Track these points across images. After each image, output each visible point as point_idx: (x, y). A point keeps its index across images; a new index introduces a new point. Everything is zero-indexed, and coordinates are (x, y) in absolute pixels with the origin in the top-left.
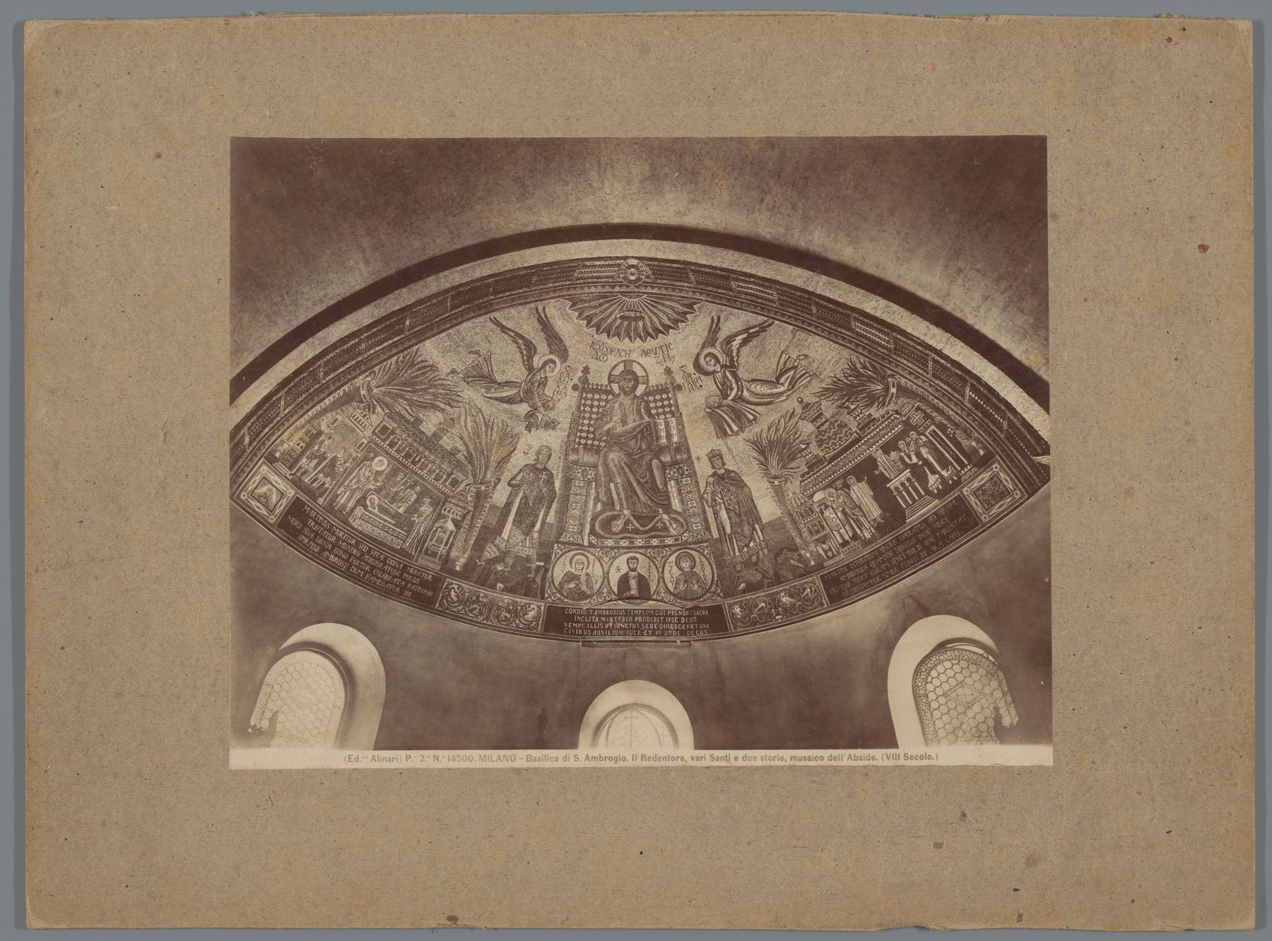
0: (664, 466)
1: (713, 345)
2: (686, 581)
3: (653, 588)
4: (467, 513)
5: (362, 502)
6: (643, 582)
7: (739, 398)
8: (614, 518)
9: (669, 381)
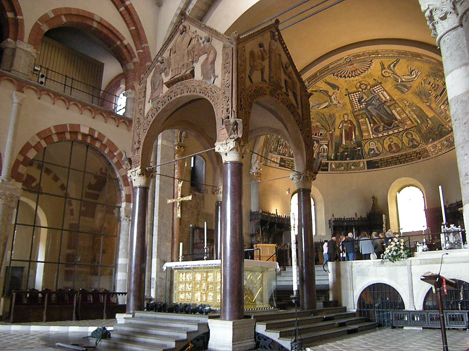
0: (389, 106)
2: (411, 142)
3: (400, 145)
4: (329, 142)
6: (397, 145)
7: (402, 81)
8: (379, 127)
9: (376, 82)
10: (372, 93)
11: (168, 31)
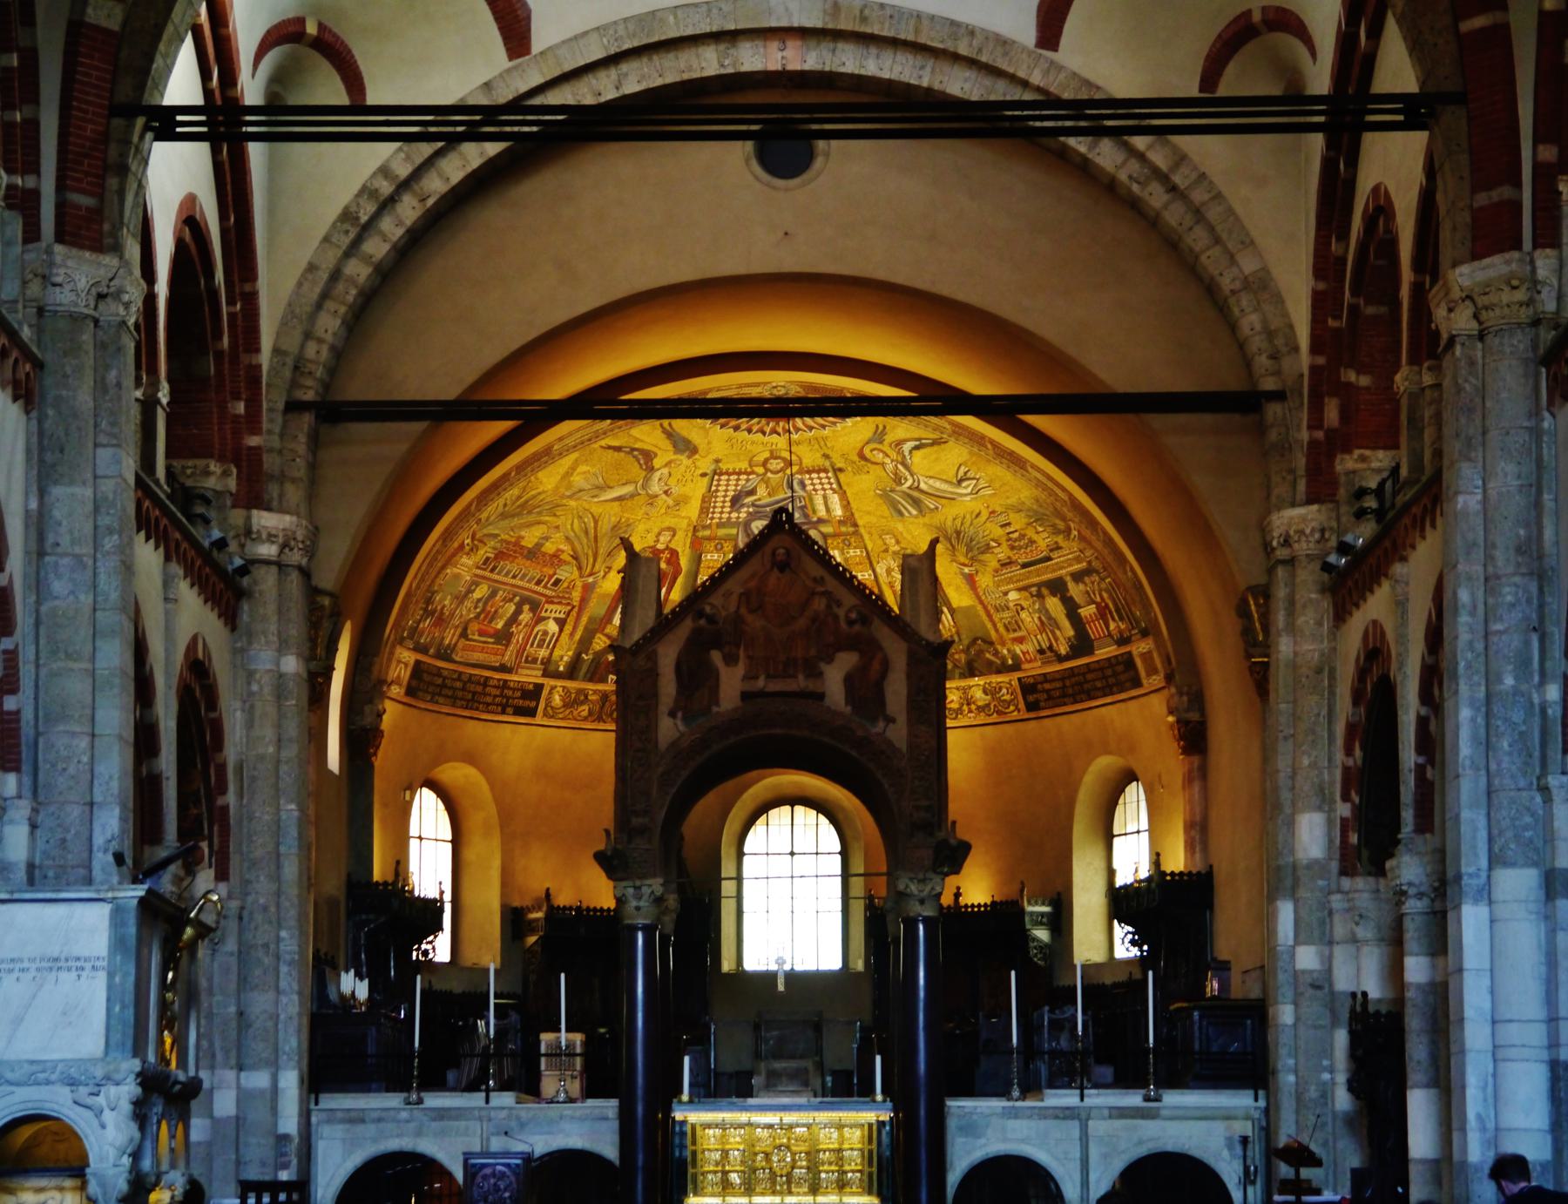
1: (881, 442)
5: (464, 635)
10: (791, 487)
11: (326, 239)
